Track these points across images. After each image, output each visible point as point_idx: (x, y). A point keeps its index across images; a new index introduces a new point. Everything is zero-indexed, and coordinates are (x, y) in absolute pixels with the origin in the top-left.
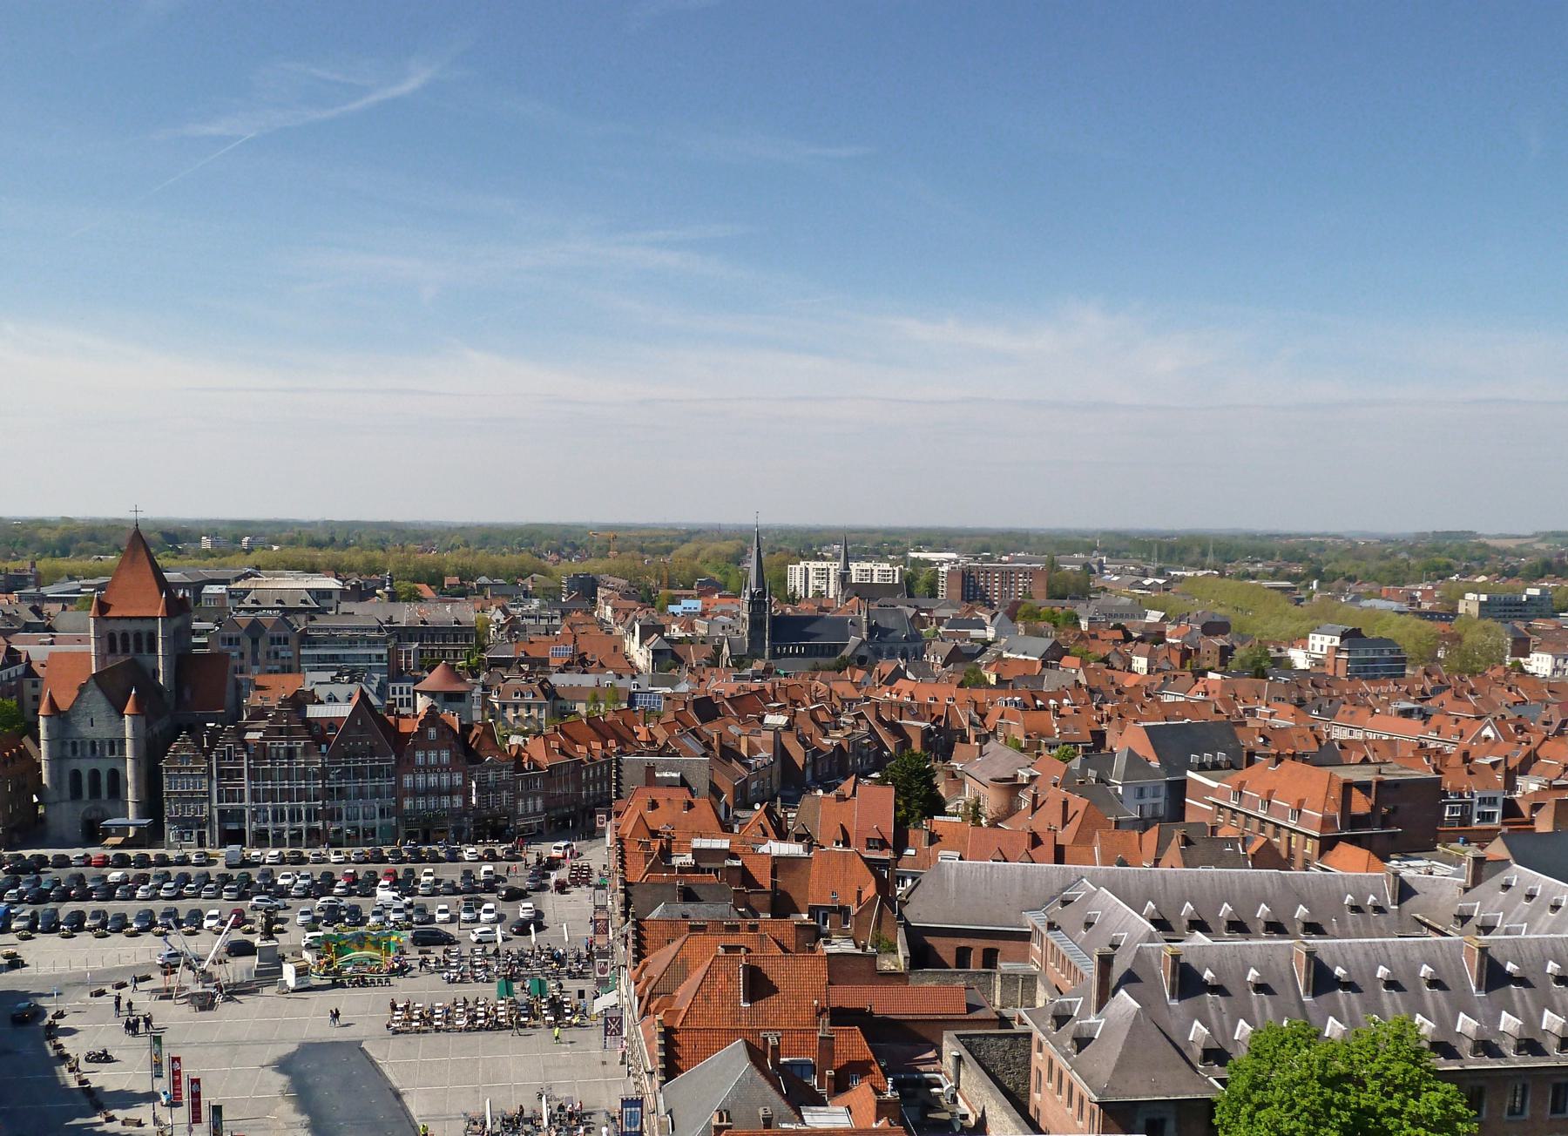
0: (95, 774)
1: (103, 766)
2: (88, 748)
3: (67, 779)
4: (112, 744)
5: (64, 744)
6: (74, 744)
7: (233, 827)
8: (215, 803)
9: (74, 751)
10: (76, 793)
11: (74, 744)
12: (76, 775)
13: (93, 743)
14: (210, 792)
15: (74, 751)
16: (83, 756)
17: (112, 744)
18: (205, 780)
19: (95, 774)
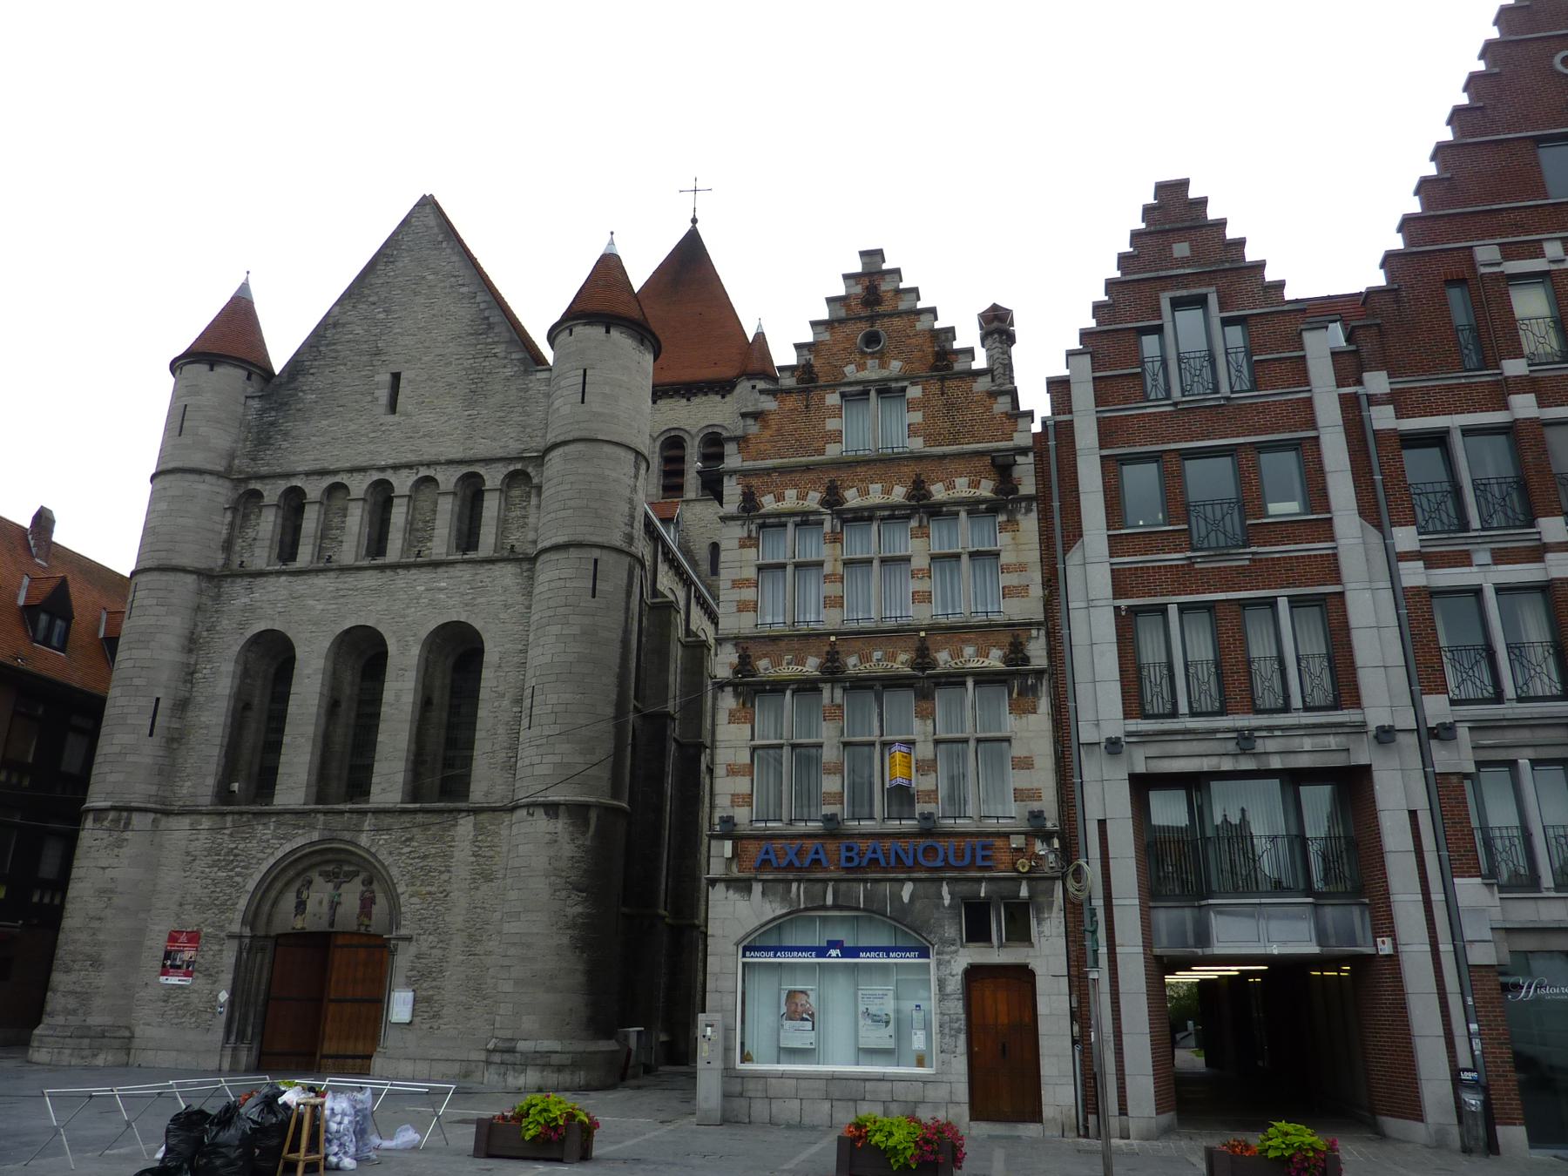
0: (363, 653)
1: (407, 611)
2: (356, 520)
3: (221, 681)
4: (472, 491)
5: (247, 502)
6: (294, 502)
7: (1258, 934)
8: (1100, 704)
9: (287, 549)
10: (249, 775)
11: (294, 502)
12: (272, 656)
13: (382, 496)
14: (1053, 621)
15: (287, 549)
16: (325, 565)
17: (472, 491)
18: (1021, 541)
19: (363, 653)
